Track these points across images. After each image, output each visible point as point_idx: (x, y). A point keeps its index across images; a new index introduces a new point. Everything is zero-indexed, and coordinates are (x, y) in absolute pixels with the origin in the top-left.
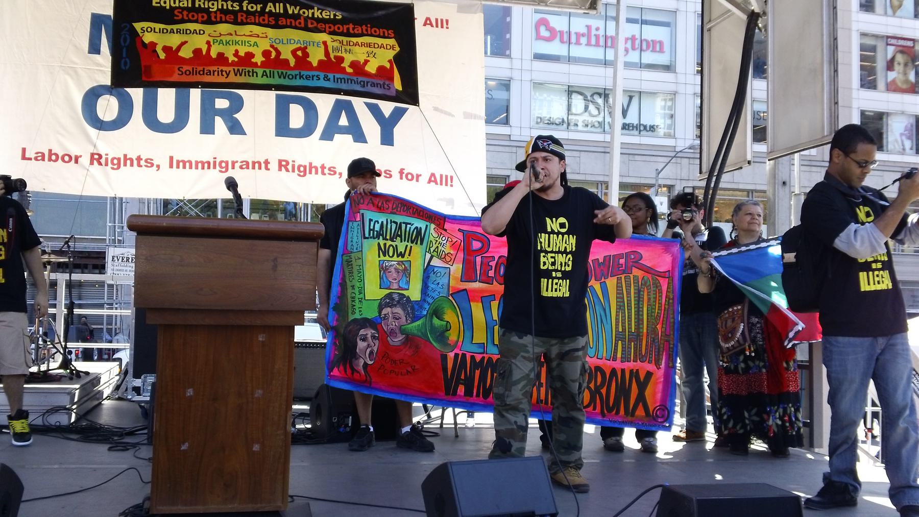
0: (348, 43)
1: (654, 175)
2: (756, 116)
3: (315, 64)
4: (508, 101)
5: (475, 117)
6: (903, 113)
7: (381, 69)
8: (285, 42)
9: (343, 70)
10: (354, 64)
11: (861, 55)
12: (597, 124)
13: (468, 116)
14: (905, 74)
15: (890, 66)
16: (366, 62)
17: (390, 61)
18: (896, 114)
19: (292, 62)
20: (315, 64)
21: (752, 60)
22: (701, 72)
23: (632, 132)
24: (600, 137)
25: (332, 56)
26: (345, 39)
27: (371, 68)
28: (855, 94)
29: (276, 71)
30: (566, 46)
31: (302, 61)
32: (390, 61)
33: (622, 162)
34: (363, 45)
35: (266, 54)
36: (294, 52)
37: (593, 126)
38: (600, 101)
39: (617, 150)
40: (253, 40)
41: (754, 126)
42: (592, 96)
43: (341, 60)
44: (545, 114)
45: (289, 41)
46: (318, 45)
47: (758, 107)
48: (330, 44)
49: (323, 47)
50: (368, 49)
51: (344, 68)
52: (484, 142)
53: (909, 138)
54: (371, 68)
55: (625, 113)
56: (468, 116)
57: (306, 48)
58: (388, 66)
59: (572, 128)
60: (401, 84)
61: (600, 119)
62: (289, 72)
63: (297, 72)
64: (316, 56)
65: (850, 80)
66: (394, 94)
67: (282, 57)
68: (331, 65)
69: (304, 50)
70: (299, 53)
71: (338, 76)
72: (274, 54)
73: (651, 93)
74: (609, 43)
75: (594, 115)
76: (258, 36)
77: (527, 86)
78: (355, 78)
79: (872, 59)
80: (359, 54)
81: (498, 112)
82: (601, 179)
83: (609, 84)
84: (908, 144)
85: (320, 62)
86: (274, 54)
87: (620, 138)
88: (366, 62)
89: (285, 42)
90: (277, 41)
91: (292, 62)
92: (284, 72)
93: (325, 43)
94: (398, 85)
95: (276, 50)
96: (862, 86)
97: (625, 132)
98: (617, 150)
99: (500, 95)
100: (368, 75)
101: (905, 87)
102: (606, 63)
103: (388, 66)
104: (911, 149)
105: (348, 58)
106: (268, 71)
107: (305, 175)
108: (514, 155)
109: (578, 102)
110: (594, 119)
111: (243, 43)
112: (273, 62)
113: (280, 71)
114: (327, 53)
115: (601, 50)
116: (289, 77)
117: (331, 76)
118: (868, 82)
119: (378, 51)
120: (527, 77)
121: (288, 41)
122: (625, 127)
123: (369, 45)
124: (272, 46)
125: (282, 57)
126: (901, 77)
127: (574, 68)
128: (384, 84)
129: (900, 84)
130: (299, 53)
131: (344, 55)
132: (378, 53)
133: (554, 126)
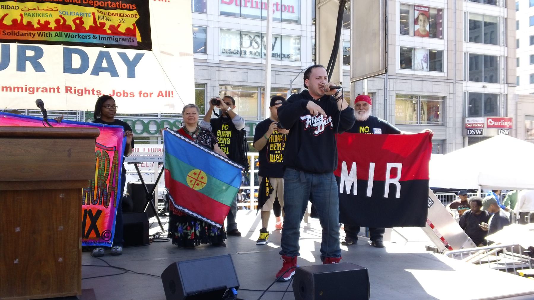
0: (108, 14)
1: (289, 83)
2: (345, 50)
3: (87, 28)
4: (206, 39)
5: (187, 55)
6: (423, 48)
7: (128, 29)
8: (69, 13)
9: (105, 32)
10: (112, 27)
11: (401, 16)
12: (257, 54)
13: (182, 54)
14: (424, 26)
15: (416, 22)
16: (119, 25)
17: (134, 25)
18: (419, 48)
19: (73, 27)
20: (87, 28)
21: (342, 20)
22: (315, 24)
23: (277, 58)
24: (259, 61)
25: (98, 23)
26: (106, 11)
27: (122, 29)
28: (397, 37)
29: (63, 33)
30: (238, 8)
31: (80, 27)
32: (134, 25)
33: (272, 76)
34: (117, 15)
35: (57, 21)
36: (74, 21)
37: (255, 54)
38: (259, 40)
39: (269, 69)
40: (49, 13)
41: (344, 56)
42: (254, 38)
43: (103, 25)
44: (227, 48)
45: (71, 14)
46: (89, 15)
47: (346, 45)
48: (97, 15)
49: (92, 16)
50: (120, 18)
51: (106, 30)
52: (193, 63)
53: (426, 62)
54: (122, 29)
55: (273, 49)
56: (182, 54)
57: (82, 18)
58: (132, 27)
59: (243, 55)
60: (142, 37)
61: (259, 50)
62: (72, 33)
63: (77, 34)
64: (88, 23)
65: (395, 30)
66: (137, 44)
67: (67, 23)
68: (97, 29)
69: (80, 19)
70: (78, 21)
71: (101, 36)
72: (62, 22)
73: (287, 36)
74: (264, 7)
75: (255, 48)
76: (52, 10)
77: (217, 31)
78: (112, 36)
79: (407, 18)
80: (115, 21)
81: (201, 46)
82: (260, 85)
83: (264, 31)
84: (425, 65)
85: (91, 27)
86: (62, 22)
87: (271, 62)
88: (119, 25)
89: (69, 13)
90: (64, 13)
91: (73, 27)
92: (69, 33)
93: (93, 14)
94: (139, 39)
95: (63, 18)
96: (401, 33)
97: (274, 58)
98: (269, 69)
99: (201, 36)
100: (121, 34)
101: (424, 33)
102: (262, 18)
103: (132, 27)
104: (427, 68)
105: (108, 24)
106: (58, 32)
107: (82, 95)
108: (210, 71)
109: (246, 40)
110: (255, 51)
111: (43, 15)
112: (62, 26)
113: (66, 33)
114: (95, 21)
115: (259, 10)
116: (71, 36)
117: (97, 36)
118: (405, 31)
119: (127, 19)
120: (216, 25)
121: (71, 13)
122: (274, 55)
123: (120, 15)
124: (61, 16)
125: (67, 23)
126: (422, 28)
127: (244, 21)
128: (130, 39)
129: (421, 32)
130: (78, 21)
131: (105, 21)
132: (127, 20)
133: (233, 55)
